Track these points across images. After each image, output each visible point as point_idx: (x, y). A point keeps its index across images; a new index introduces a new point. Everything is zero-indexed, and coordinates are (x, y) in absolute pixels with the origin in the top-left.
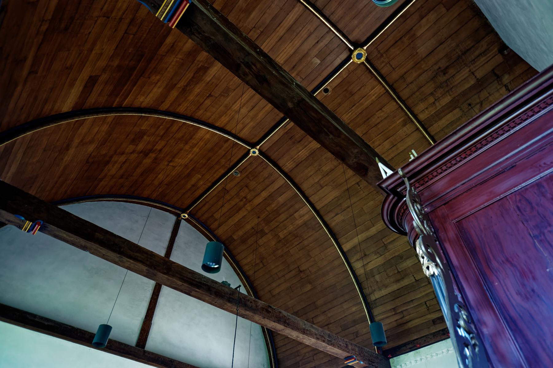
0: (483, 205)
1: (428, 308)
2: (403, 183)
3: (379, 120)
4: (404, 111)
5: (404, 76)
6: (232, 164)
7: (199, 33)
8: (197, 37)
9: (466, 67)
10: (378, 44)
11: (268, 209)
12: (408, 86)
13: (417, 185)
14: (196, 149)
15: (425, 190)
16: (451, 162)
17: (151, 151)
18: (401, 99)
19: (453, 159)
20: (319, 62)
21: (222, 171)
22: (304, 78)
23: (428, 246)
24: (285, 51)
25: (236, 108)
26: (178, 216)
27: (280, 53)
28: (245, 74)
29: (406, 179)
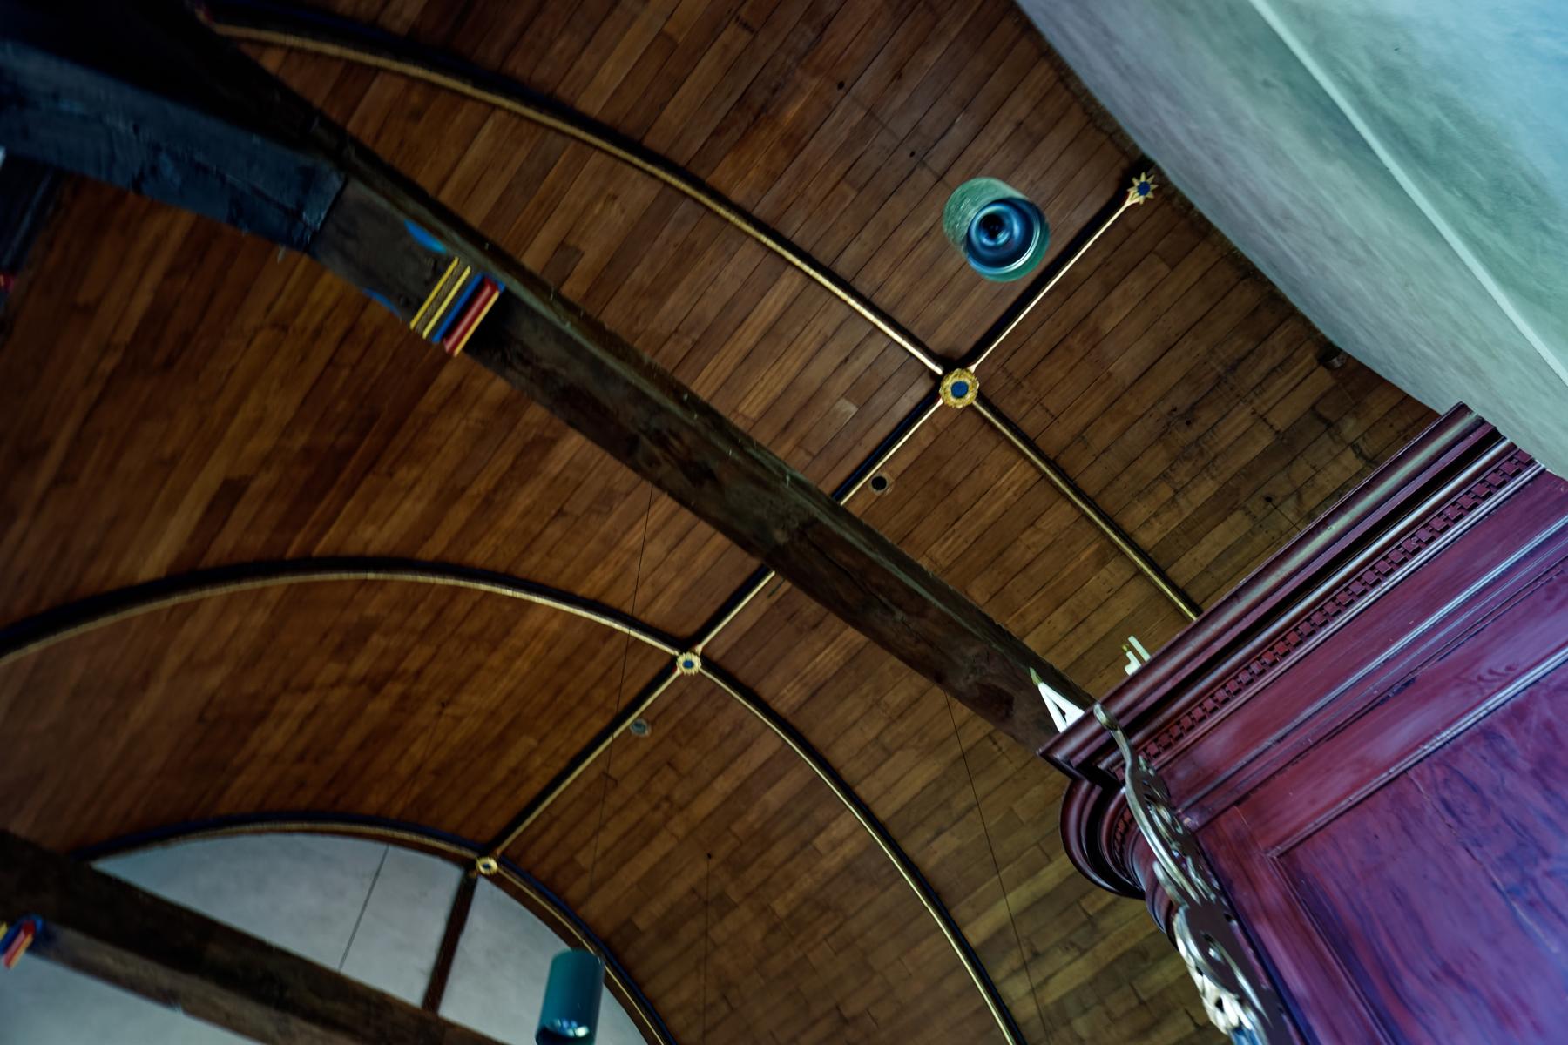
0: (1348, 800)
2: (1111, 745)
3: (1029, 556)
4: (1096, 525)
5: (1084, 434)
6: (625, 700)
7: (527, 363)
8: (521, 373)
9: (1241, 404)
10: (1006, 356)
11: (736, 828)
12: (1097, 458)
13: (1153, 749)
14: (522, 665)
15: (1176, 760)
16: (1236, 677)
17: (391, 676)
18: (1085, 493)
19: (1241, 668)
20: (853, 409)
21: (599, 724)
22: (815, 452)
23: (1209, 939)
24: (761, 386)
26: (468, 866)
27: (749, 392)
28: (653, 461)
29: (1119, 732)
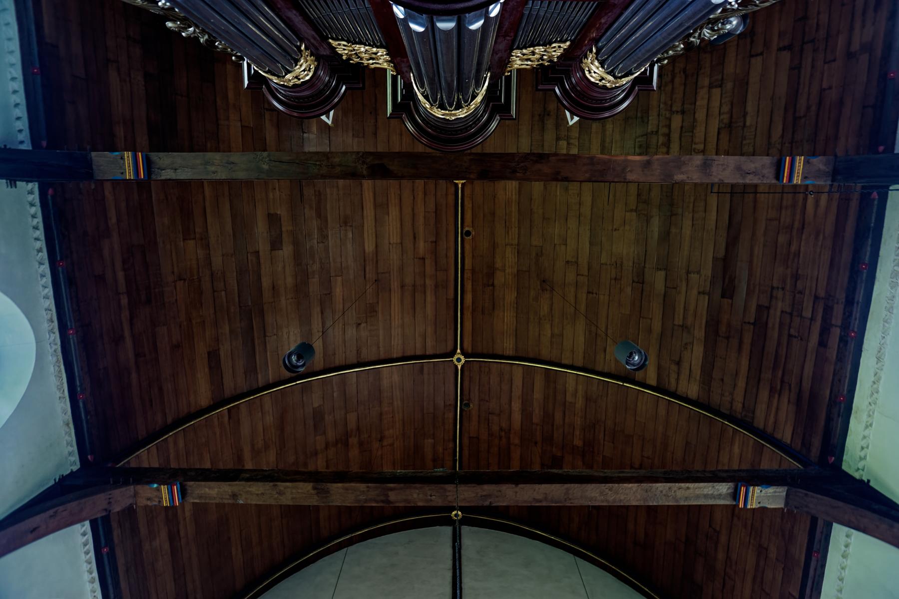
1: (799, 338)
25: (397, 322)
